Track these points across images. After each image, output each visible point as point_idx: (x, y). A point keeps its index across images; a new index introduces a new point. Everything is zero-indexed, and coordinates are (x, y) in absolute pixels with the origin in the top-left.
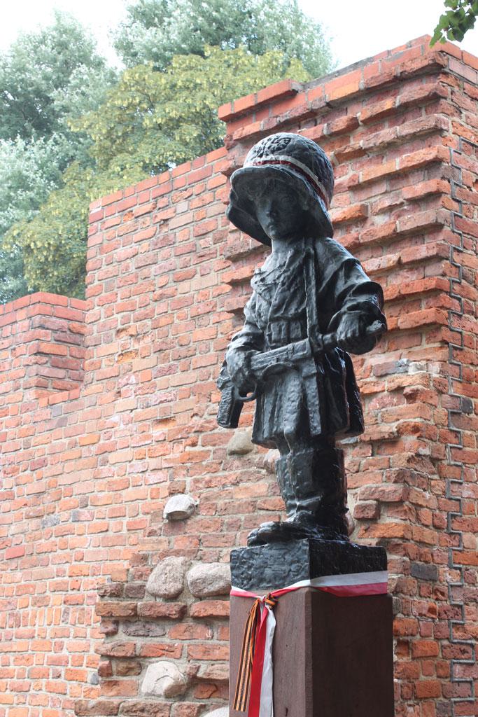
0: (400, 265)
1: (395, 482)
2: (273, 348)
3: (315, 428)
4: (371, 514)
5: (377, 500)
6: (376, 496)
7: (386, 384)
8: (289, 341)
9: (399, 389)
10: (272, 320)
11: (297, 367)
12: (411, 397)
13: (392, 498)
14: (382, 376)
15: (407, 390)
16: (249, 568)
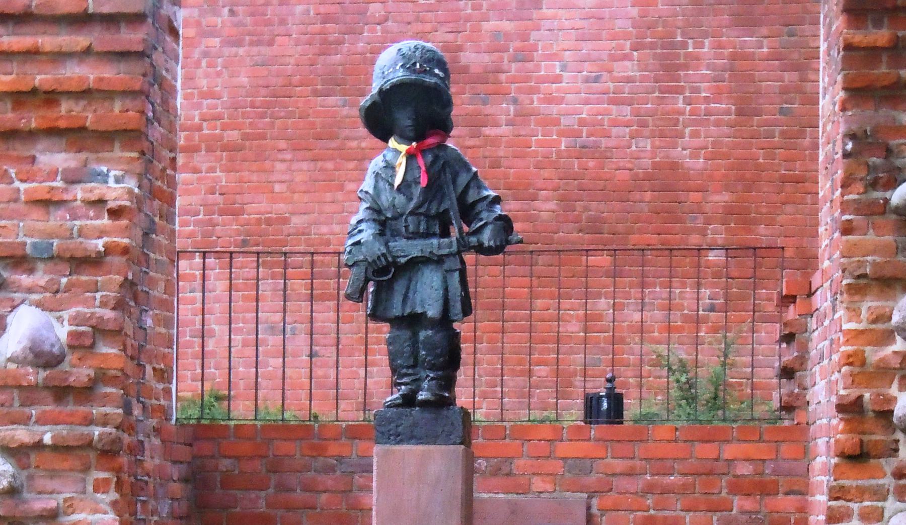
0: (87, 52)
1: (114, 309)
2: (408, 238)
3: (457, 315)
4: (88, 342)
5: (93, 327)
6: (93, 322)
7: (79, 192)
8: (427, 235)
9: (101, 202)
10: (412, 213)
11: (439, 261)
12: (115, 213)
13: (111, 326)
14: (73, 182)
15: (111, 205)
16: (397, 426)
